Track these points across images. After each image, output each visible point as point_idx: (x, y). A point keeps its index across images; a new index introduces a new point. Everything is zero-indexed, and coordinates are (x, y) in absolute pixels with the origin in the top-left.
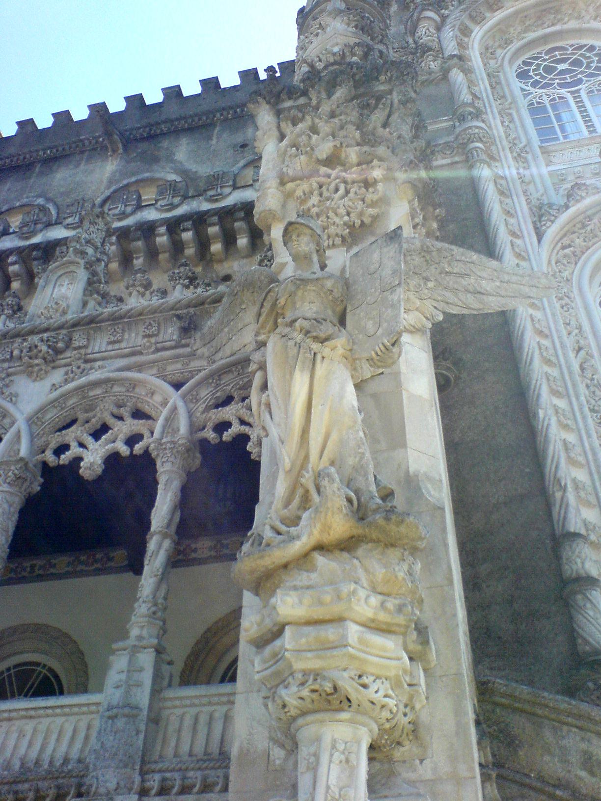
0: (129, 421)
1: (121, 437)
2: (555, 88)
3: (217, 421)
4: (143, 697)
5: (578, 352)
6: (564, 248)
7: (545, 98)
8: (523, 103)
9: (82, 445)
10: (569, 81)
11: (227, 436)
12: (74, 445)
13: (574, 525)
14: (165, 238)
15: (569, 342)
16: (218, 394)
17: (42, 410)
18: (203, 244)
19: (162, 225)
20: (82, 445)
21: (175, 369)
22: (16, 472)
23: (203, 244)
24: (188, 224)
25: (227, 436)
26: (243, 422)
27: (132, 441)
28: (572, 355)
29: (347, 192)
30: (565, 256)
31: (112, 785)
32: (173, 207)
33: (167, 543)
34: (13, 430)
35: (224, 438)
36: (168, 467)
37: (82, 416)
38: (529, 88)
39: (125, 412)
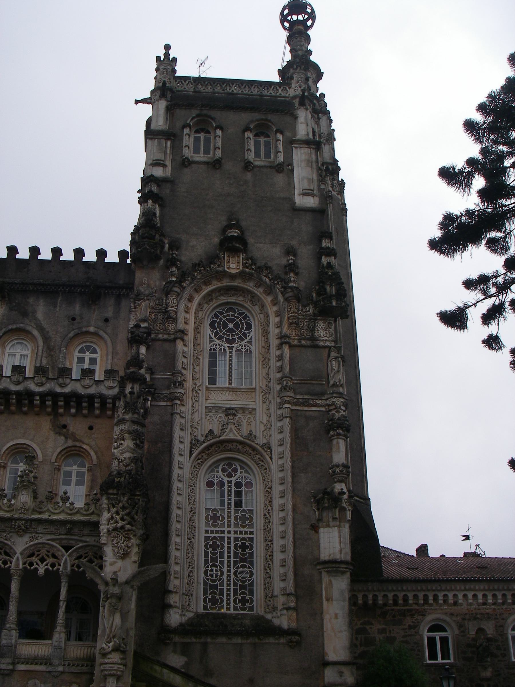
2: (223, 341)
4: (63, 644)
5: (190, 512)
6: (198, 459)
7: (218, 346)
8: (208, 347)
9: (37, 564)
10: (231, 338)
13: (171, 587)
14: (38, 402)
15: (188, 509)
17: (24, 550)
18: (55, 406)
19: (37, 395)
20: (37, 564)
21: (65, 543)
23: (55, 406)
24: (49, 398)
27: (53, 565)
28: (188, 513)
29: (124, 540)
30: (198, 463)
31: (58, 663)
32: (42, 385)
33: (65, 603)
34: (16, 556)
37: (36, 553)
38: (213, 337)
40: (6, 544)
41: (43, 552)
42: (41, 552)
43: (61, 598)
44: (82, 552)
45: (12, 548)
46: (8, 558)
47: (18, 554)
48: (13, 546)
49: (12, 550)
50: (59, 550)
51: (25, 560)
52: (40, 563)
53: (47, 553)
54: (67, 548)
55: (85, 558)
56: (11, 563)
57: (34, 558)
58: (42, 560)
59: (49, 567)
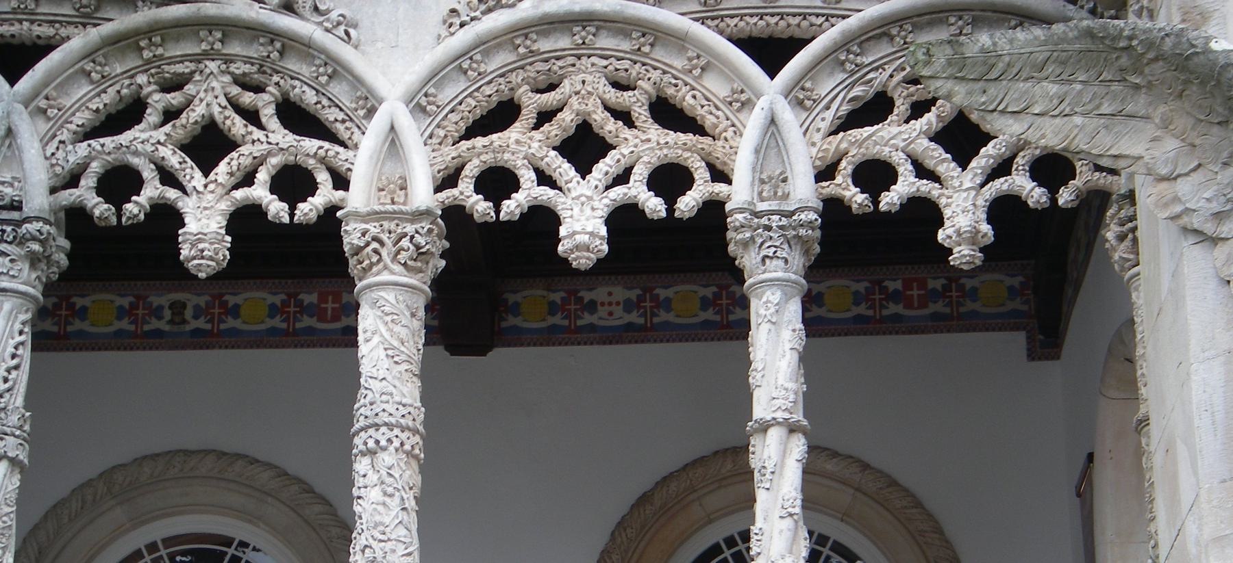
0: (655, 133)
1: (640, 173)
3: (858, 159)
9: (544, 179)
11: (891, 199)
12: (527, 177)
16: (857, 91)
17: (436, 76)
22: (420, 240)
25: (891, 199)
26: (922, 172)
27: (670, 179)
33: (798, 447)
34: (377, 126)
35: (883, 206)
36: (775, 270)
37: (531, 103)
39: (637, 103)
40: (289, 44)
41: (584, 94)
42: (566, 87)
43: (760, 410)
44: (883, 71)
45: (337, 70)
46: (311, 144)
47: (394, 109)
48: (345, 52)
49: (339, 90)
50: (709, 63)
51: (449, 154)
52: (564, 169)
53: (612, 95)
54: (770, 52)
55: (919, 109)
56: (341, 181)
57: (513, 134)
58: (584, 148)
59: (638, 191)
